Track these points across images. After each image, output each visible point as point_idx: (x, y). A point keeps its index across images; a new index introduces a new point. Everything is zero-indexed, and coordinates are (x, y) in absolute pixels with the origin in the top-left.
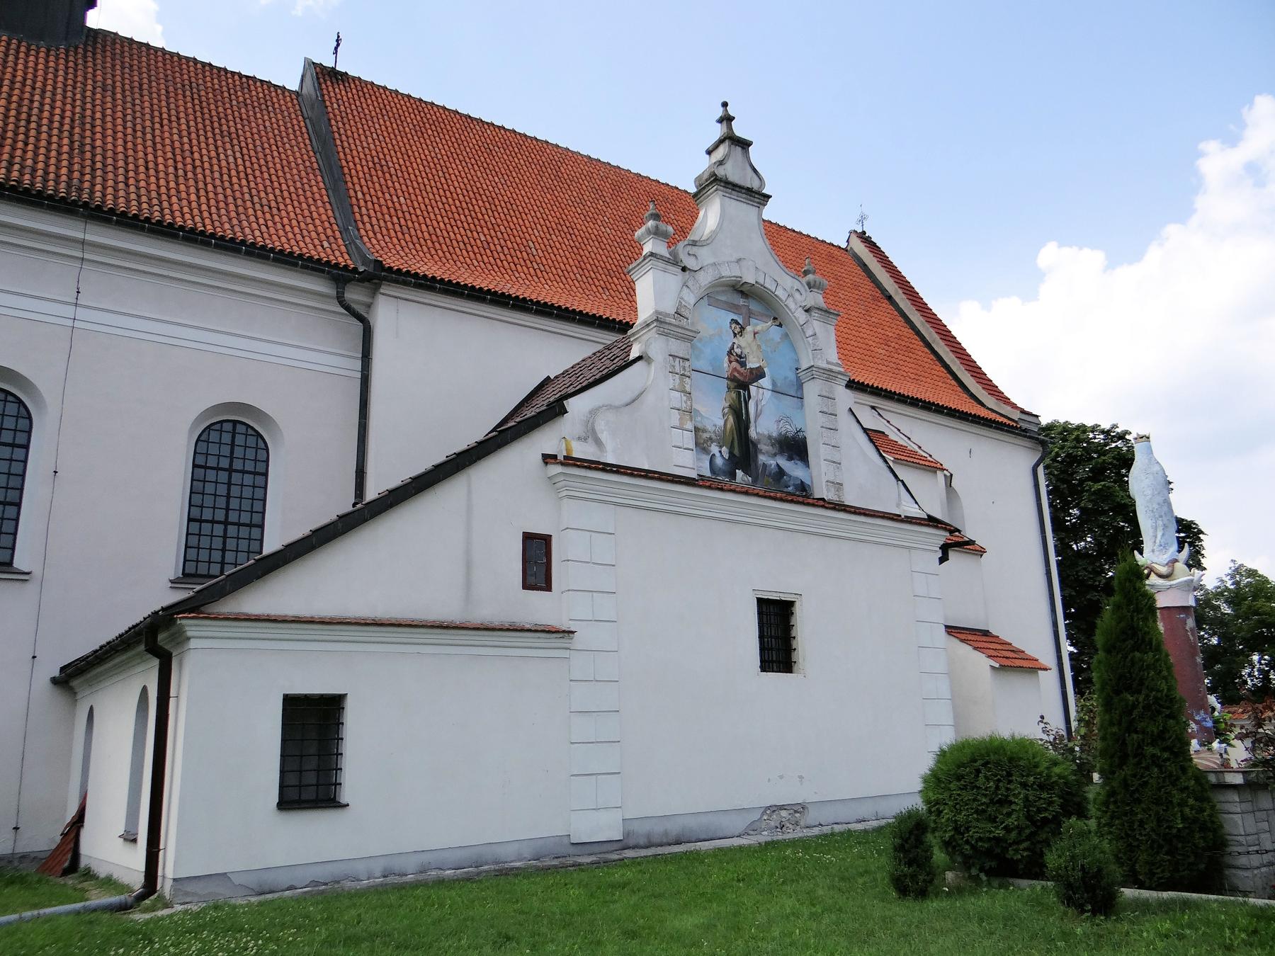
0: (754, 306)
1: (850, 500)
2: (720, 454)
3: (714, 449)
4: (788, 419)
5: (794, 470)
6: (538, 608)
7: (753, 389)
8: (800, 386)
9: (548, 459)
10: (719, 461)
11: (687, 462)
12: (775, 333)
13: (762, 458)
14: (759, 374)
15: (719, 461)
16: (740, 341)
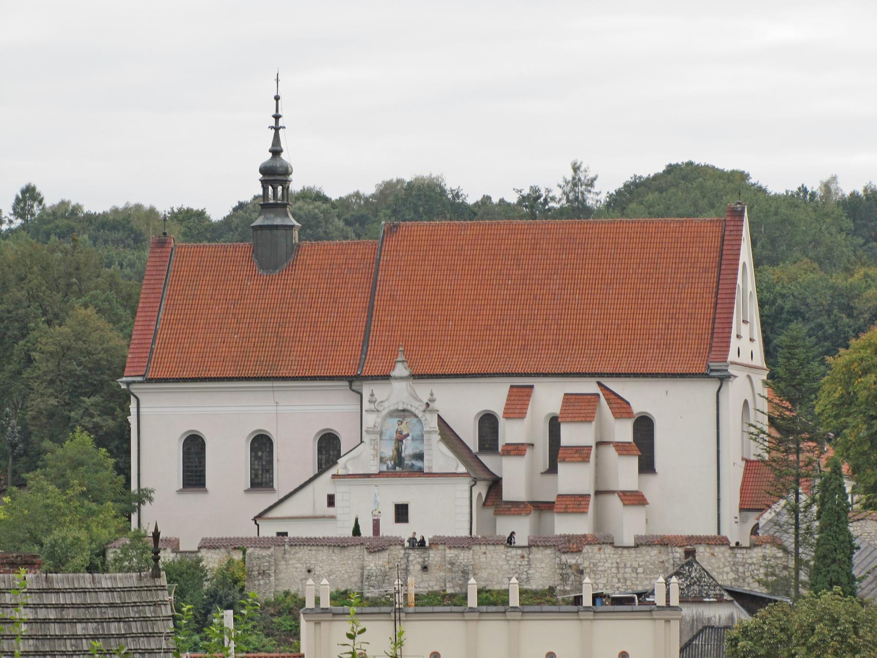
0: (406, 414)
1: (434, 471)
2: (390, 464)
3: (389, 462)
4: (417, 448)
5: (418, 464)
6: (331, 511)
7: (404, 441)
8: (423, 436)
9: (333, 475)
10: (390, 466)
11: (374, 470)
12: (415, 420)
13: (406, 462)
14: (408, 435)
15: (390, 466)
16: (401, 426)
